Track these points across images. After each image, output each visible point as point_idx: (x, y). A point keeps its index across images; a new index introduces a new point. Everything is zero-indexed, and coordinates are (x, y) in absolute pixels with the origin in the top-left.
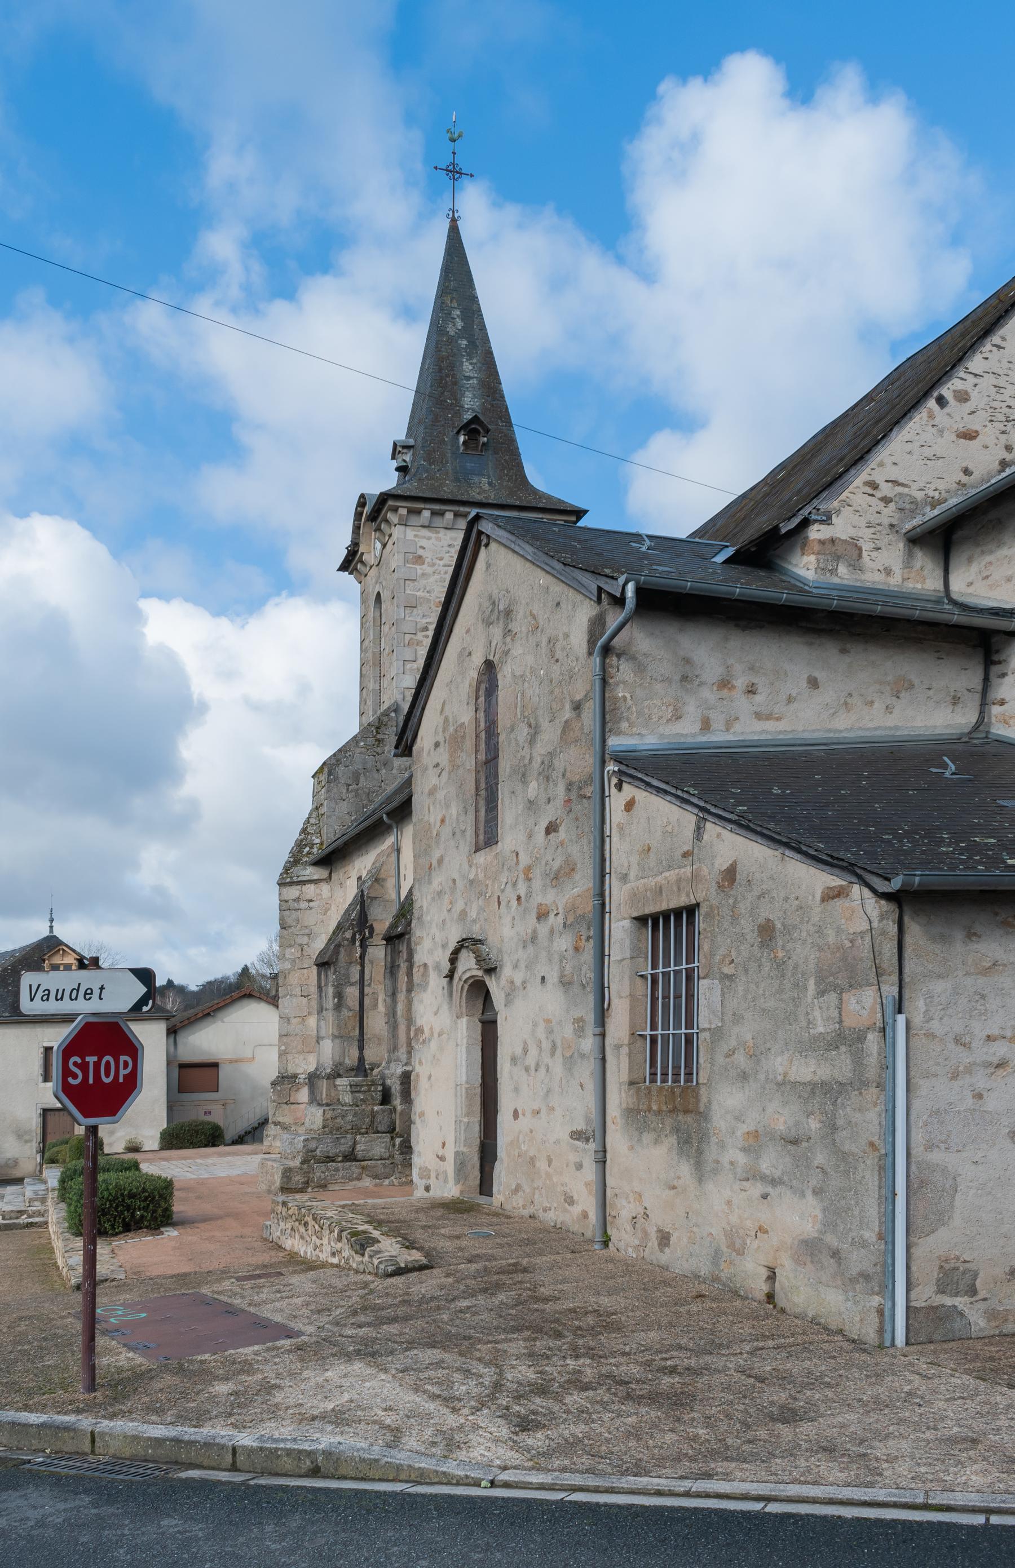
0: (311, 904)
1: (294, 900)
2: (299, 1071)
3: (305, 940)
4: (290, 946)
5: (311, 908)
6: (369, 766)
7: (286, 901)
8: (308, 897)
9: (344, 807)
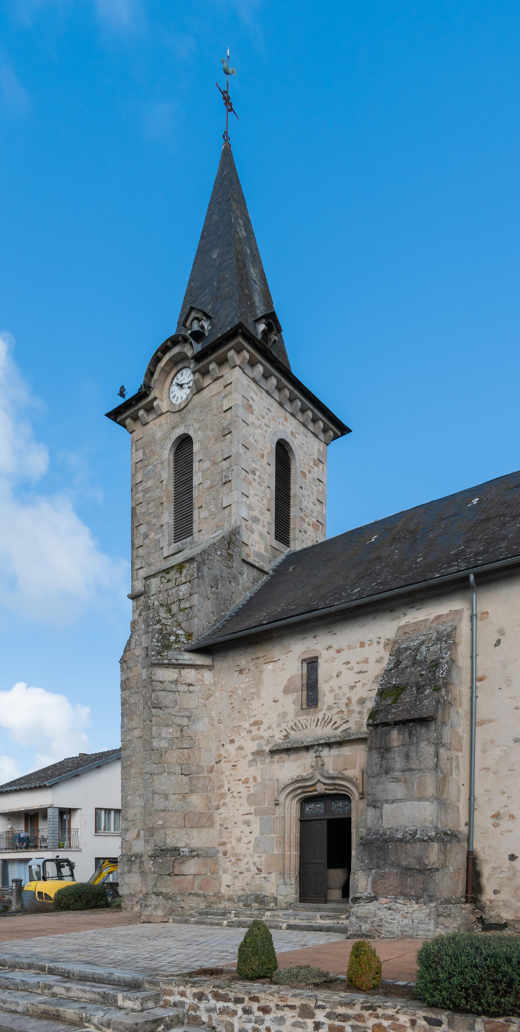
0: (191, 688)
1: (172, 682)
2: (180, 844)
3: (185, 721)
4: (167, 726)
6: (224, 576)
7: (161, 682)
8: (188, 681)
9: (209, 606)
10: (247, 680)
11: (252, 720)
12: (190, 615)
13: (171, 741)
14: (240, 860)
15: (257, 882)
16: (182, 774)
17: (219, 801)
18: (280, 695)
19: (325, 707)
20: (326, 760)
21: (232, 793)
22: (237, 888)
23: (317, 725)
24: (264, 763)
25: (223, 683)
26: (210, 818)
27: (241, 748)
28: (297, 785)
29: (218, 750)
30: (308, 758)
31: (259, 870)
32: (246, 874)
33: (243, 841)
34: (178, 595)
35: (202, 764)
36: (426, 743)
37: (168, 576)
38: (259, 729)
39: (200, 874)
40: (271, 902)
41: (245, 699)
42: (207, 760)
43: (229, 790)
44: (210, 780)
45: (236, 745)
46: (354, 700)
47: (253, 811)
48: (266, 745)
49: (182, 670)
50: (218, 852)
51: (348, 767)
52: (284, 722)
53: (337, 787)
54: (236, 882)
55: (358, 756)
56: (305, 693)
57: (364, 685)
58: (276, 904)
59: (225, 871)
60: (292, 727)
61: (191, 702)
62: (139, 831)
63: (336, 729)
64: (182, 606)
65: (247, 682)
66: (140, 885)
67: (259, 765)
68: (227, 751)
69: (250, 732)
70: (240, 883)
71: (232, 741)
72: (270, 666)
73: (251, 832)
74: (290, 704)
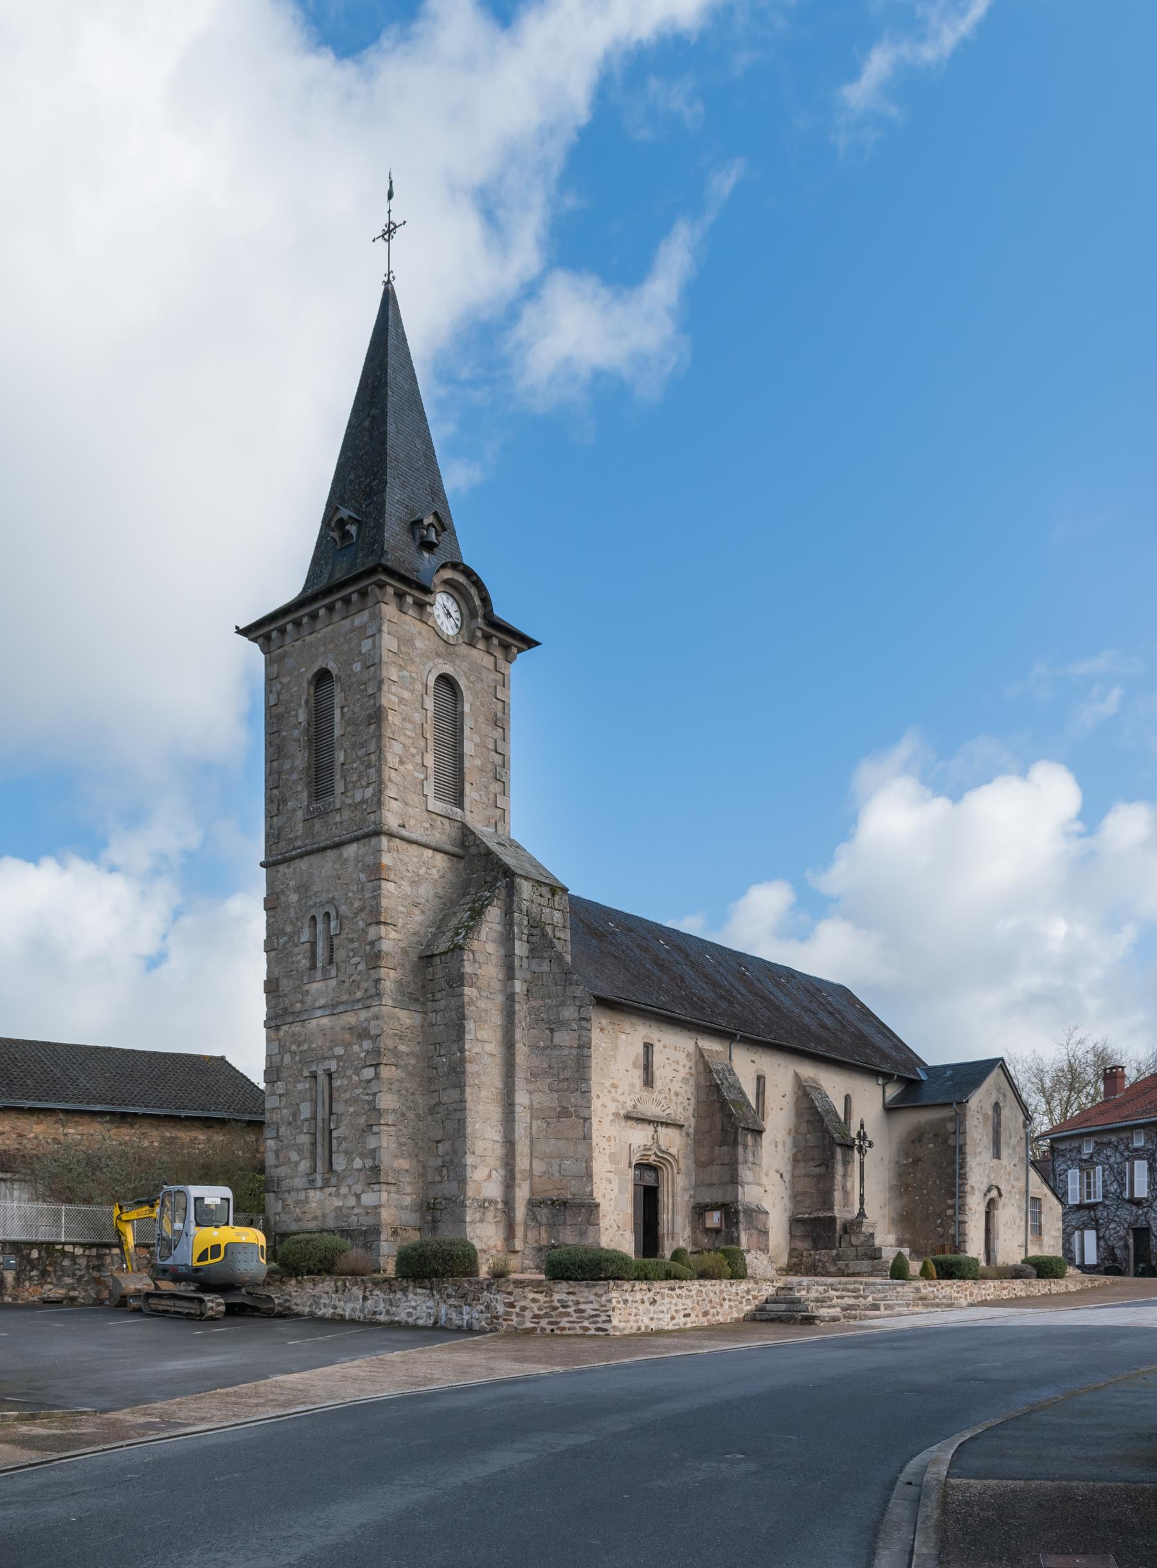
11: (612, 1081)
18: (630, 1067)
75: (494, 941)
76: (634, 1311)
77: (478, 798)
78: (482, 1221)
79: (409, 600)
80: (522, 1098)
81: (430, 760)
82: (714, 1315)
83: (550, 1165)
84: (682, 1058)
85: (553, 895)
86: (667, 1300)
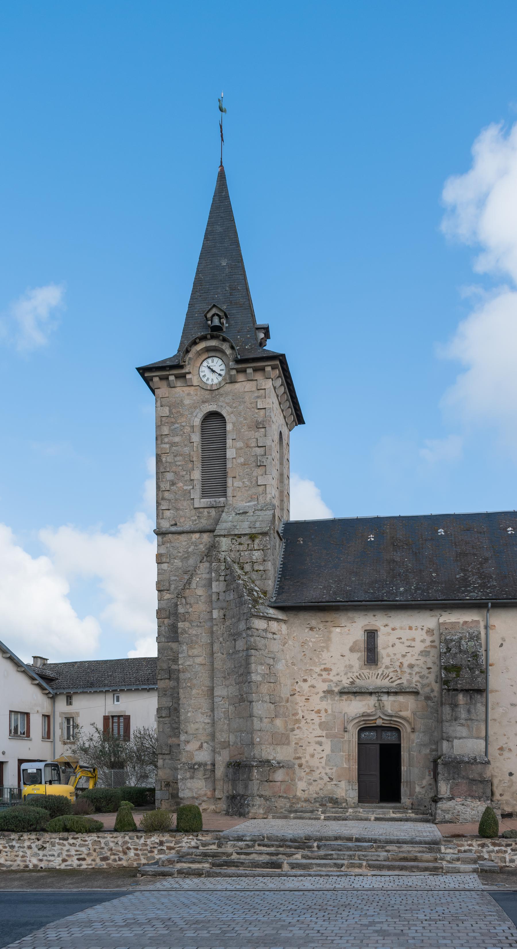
0: (275, 636)
1: (263, 631)
2: (270, 758)
3: (271, 662)
4: (261, 664)
5: (275, 639)
7: (257, 630)
8: (273, 631)
10: (317, 636)
11: (323, 667)
12: (264, 576)
13: (263, 676)
14: (314, 771)
15: (329, 788)
16: (270, 703)
17: (294, 725)
18: (347, 652)
19: (384, 666)
20: (385, 703)
21: (306, 719)
22: (311, 792)
23: (377, 678)
24: (334, 700)
25: (295, 635)
26: (288, 738)
27: (314, 687)
28: (363, 719)
29: (292, 685)
30: (372, 700)
31: (331, 779)
32: (319, 781)
33: (316, 756)
34: (251, 558)
35: (282, 695)
36: (480, 704)
37: (239, 540)
38: (329, 674)
39: (285, 781)
40: (344, 802)
41: (315, 650)
42: (285, 692)
43: (303, 717)
44: (287, 709)
45: (309, 683)
46: (406, 664)
47: (324, 735)
48: (335, 687)
49: (269, 622)
50: (294, 764)
51: (402, 710)
52: (350, 672)
53: (392, 722)
54: (311, 787)
55: (409, 703)
56: (366, 653)
57: (412, 655)
58: (347, 804)
59: (301, 779)
60: (357, 676)
61: (275, 646)
62: (202, 743)
63: (392, 682)
64: (256, 568)
65: (317, 638)
66: (205, 789)
67: (329, 701)
68: (301, 687)
69: (321, 675)
70: (314, 788)
71: (305, 681)
72: (338, 630)
73: (323, 751)
74: (356, 660)
75: (204, 586)
76: (21, 854)
77: (240, 484)
78: (192, 778)
79: (172, 378)
80: (218, 692)
81: (197, 475)
82: (115, 860)
83: (236, 737)
84: (419, 635)
85: (253, 541)
86: (57, 847)
